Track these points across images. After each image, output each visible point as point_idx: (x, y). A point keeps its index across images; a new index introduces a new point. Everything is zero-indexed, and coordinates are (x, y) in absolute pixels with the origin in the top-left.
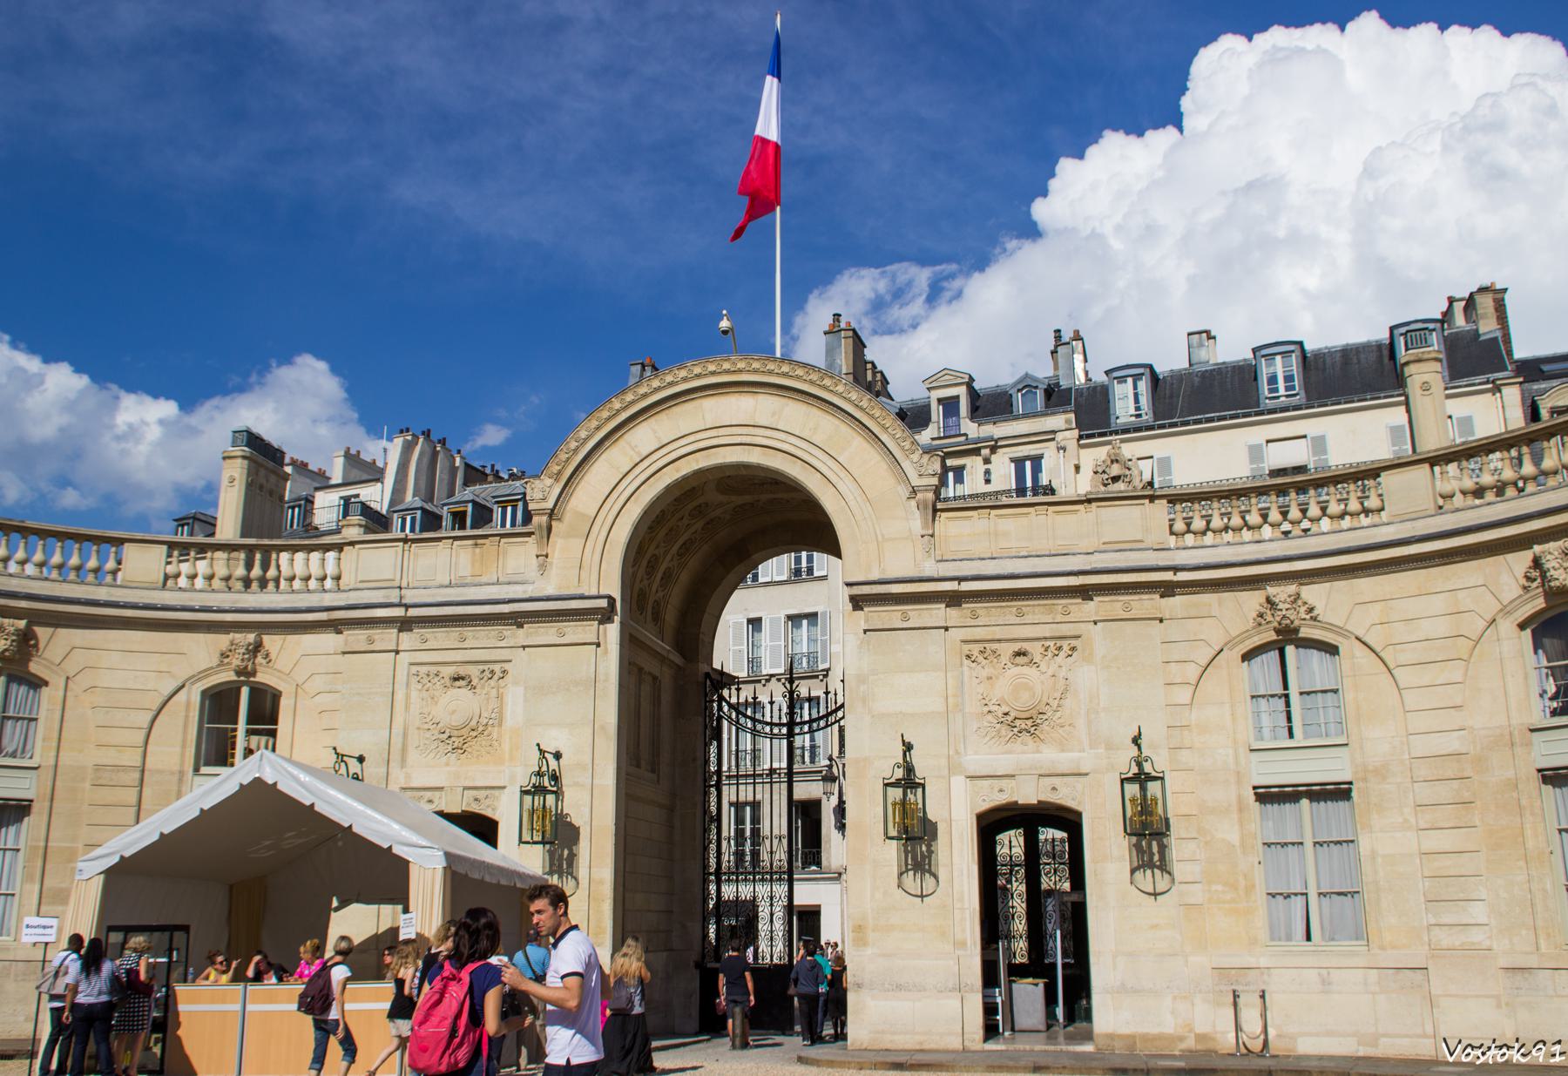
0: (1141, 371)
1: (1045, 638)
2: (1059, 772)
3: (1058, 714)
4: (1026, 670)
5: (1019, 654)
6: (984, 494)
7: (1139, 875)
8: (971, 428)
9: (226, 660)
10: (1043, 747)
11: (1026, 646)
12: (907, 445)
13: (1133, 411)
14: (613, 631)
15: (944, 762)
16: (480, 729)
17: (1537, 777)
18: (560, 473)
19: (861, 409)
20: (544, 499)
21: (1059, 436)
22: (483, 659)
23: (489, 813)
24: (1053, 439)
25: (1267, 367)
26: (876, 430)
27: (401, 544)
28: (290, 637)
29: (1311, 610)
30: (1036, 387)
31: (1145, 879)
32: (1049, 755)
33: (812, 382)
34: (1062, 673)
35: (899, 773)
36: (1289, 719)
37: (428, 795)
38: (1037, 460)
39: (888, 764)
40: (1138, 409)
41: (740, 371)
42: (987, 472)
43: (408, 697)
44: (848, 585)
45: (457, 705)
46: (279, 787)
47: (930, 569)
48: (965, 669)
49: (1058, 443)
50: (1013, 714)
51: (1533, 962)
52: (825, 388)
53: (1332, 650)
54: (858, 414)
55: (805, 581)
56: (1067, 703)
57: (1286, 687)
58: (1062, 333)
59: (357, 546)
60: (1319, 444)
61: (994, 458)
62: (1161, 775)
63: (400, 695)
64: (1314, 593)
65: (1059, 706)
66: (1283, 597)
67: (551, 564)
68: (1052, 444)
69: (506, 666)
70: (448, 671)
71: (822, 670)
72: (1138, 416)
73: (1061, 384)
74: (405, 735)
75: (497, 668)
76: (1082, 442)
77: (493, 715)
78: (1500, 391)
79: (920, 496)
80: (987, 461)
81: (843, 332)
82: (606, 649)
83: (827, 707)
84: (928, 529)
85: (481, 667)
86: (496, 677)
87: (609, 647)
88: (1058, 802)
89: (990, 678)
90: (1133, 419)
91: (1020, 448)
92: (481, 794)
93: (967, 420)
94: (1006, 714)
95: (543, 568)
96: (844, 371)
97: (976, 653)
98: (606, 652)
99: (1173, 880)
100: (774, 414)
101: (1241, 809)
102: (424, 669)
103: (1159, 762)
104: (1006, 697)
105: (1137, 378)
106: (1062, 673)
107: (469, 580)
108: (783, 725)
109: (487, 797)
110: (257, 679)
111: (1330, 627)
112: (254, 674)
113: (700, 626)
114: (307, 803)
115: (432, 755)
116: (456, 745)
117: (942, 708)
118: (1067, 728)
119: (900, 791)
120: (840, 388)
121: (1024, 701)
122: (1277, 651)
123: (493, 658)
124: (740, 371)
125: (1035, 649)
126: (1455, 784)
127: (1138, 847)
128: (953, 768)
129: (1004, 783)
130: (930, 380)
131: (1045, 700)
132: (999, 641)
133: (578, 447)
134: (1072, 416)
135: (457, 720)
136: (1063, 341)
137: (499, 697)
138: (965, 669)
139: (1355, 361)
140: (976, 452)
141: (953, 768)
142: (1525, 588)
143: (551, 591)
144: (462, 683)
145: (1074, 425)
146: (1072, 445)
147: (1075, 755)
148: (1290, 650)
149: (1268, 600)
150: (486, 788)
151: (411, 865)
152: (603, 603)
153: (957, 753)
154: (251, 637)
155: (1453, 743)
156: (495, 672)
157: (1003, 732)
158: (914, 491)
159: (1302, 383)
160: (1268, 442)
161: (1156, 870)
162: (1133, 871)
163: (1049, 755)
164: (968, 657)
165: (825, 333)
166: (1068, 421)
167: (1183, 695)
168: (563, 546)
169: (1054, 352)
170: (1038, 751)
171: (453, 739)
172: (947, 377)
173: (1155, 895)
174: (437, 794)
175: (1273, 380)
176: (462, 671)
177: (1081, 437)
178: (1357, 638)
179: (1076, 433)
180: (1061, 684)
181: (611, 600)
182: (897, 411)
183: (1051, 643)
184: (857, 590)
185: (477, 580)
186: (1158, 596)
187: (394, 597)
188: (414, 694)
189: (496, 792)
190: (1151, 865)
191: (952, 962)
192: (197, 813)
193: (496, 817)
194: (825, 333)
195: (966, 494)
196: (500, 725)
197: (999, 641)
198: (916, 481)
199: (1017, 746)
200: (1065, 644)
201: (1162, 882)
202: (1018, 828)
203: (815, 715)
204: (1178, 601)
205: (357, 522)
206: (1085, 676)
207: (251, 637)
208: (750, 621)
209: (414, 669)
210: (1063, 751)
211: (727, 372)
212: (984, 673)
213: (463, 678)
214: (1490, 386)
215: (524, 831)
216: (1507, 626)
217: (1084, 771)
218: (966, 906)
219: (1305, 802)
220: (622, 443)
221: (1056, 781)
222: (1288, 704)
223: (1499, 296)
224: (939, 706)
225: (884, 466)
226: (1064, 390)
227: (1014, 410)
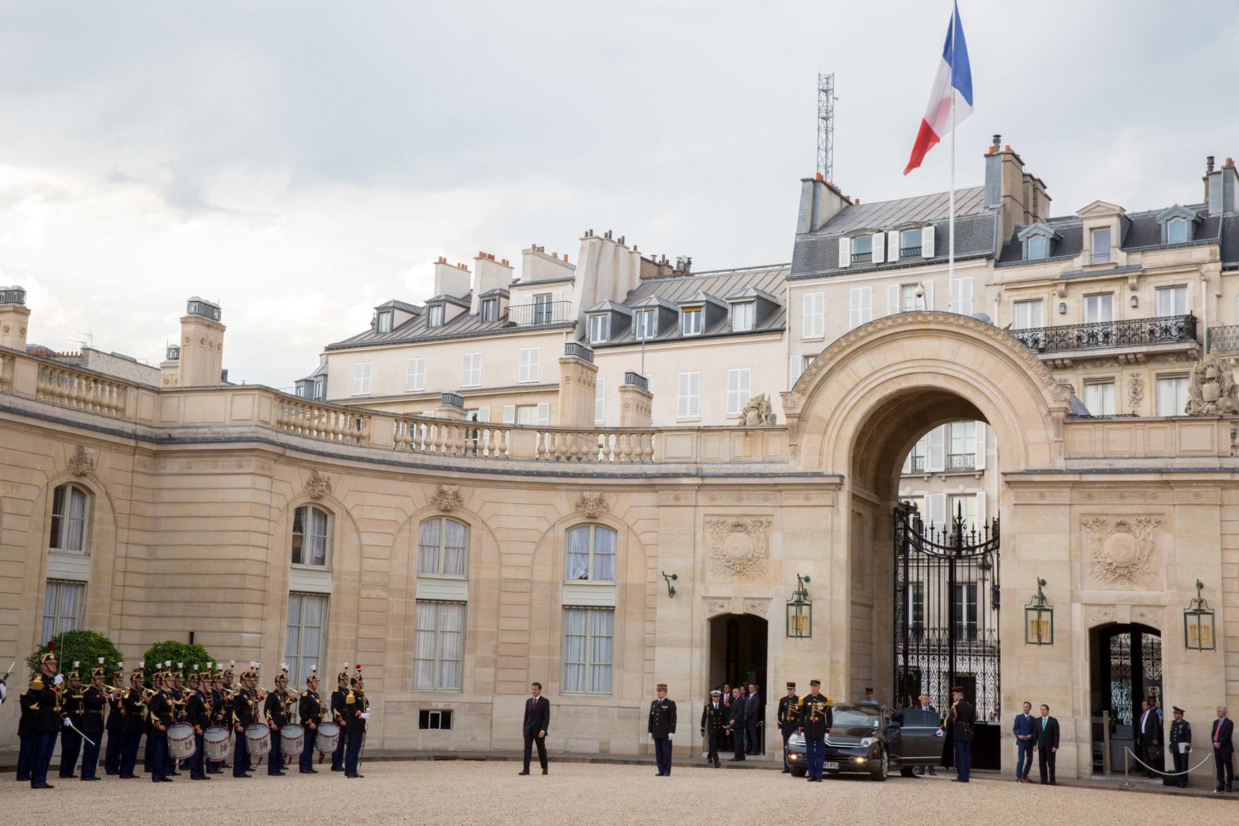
1: (1139, 515)
2: (1146, 604)
3: (1147, 566)
4: (1124, 535)
5: (1121, 524)
6: (1129, 321)
8: (1120, 257)
10: (1135, 586)
11: (1126, 519)
12: (1046, 379)
14: (843, 499)
15: (1068, 594)
16: (754, 560)
18: (805, 389)
21: (1204, 268)
22: (755, 513)
23: (761, 615)
26: (1024, 368)
27: (695, 433)
28: (621, 495)
32: (1139, 592)
33: (980, 332)
34: (1151, 538)
35: (1036, 602)
37: (720, 602)
39: (1028, 593)
41: (929, 322)
43: (704, 536)
44: (1004, 474)
45: (739, 544)
47: (1060, 464)
50: (1115, 565)
54: (1012, 356)
56: (1153, 558)
58: (1215, 160)
59: (664, 433)
62: (1212, 612)
63: (699, 536)
65: (1147, 560)
67: (800, 451)
68: (1196, 275)
69: (770, 519)
70: (731, 520)
73: (1210, 212)
74: (703, 562)
75: (764, 519)
76: (1223, 274)
77: (763, 551)
79: (1054, 414)
81: (1002, 156)
82: (838, 509)
83: (986, 538)
84: (1059, 437)
85: (754, 519)
86: (764, 526)
87: (840, 508)
88: (1145, 623)
89: (1099, 540)
91: (1166, 278)
92: (756, 603)
93: (1118, 250)
94: (1110, 564)
95: (794, 453)
96: (1003, 193)
98: (838, 511)
100: (953, 352)
103: (1213, 598)
104: (1110, 553)
106: (1151, 538)
109: (760, 604)
113: (891, 473)
115: (722, 576)
116: (738, 569)
117: (1066, 558)
118: (1152, 575)
119: (1036, 612)
120: (1000, 337)
121: (1121, 557)
123: (762, 513)
125: (1132, 521)
128: (1073, 599)
129: (1107, 610)
130: (1083, 211)
131: (1137, 555)
133: (817, 372)
135: (738, 554)
136: (1215, 170)
137: (767, 539)
138: (1083, 532)
141: (1073, 599)
143: (800, 469)
144: (739, 529)
145: (1218, 257)
146: (1215, 276)
147: (1158, 593)
150: (759, 599)
152: (837, 480)
153: (1076, 588)
154: (597, 494)
156: (764, 523)
157: (1108, 576)
158: (1050, 412)
163: (1139, 592)
165: (986, 156)
166: (1212, 253)
168: (808, 441)
169: (1205, 179)
170: (1132, 590)
171: (736, 566)
172: (1099, 209)
174: (726, 601)
176: (740, 521)
177: (1224, 269)
179: (1219, 265)
180: (1148, 548)
181: (842, 477)
182: (1052, 237)
183: (1143, 518)
184: (1009, 478)
186: (1219, 490)
187: (692, 469)
188: (708, 535)
189: (766, 602)
191: (1070, 723)
193: (766, 618)
194: (986, 156)
195: (1114, 320)
197: (1107, 515)
198: (1052, 405)
199: (1118, 585)
200: (1155, 520)
202: (1127, 633)
205: (631, 389)
206: (1166, 541)
207: (597, 494)
209: (708, 519)
210: (1149, 590)
211: (921, 322)
212: (1097, 535)
213: (742, 526)
215: (790, 629)
217: (1163, 603)
218: (1081, 688)
220: (848, 369)
221: (1144, 610)
224: (1064, 556)
226: (1211, 219)
227: (1163, 238)
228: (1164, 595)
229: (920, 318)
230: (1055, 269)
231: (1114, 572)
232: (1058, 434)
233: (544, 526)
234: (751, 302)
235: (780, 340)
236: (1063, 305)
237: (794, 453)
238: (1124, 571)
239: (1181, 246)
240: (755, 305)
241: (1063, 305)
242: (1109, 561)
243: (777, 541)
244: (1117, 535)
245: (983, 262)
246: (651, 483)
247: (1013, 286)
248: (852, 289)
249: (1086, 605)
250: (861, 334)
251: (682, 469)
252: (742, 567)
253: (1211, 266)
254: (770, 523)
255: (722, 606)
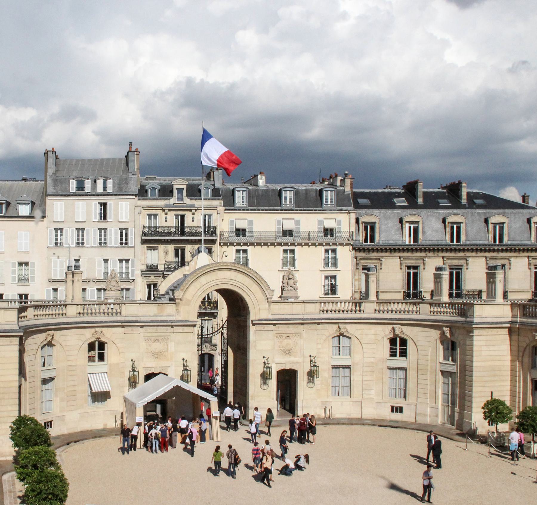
0: (245, 189)
1: (293, 333)
4: (289, 340)
7: (308, 384)
8: (187, 201)
9: (94, 336)
13: (241, 203)
17: (387, 368)
19: (257, 278)
20: (179, 296)
21: (218, 209)
24: (216, 210)
25: (284, 194)
29: (347, 330)
30: (209, 188)
31: (309, 385)
32: (292, 359)
33: (246, 270)
36: (339, 351)
38: (210, 216)
40: (243, 202)
41: (228, 266)
42: (193, 218)
45: (157, 347)
46: (181, 386)
48: (276, 339)
49: (218, 211)
51: (381, 401)
52: (249, 272)
53: (350, 338)
55: (124, 247)
57: (339, 345)
60: (298, 223)
61: (196, 213)
64: (348, 326)
66: (342, 327)
69: (169, 337)
71: (132, 280)
72: (243, 204)
75: (166, 337)
76: (225, 211)
78: (350, 214)
80: (193, 214)
89: (281, 342)
90: (241, 205)
94: (284, 350)
95: (178, 312)
96: (136, 168)
97: (278, 337)
98: (194, 334)
99: (315, 385)
101: (329, 369)
102: (147, 338)
105: (243, 191)
107: (157, 314)
108: (200, 335)
110: (101, 340)
111: (350, 334)
112: (100, 338)
114: (188, 390)
121: (288, 347)
122: (338, 337)
124: (228, 266)
125: (291, 335)
126: (371, 368)
127: (308, 378)
132: (283, 333)
134: (222, 201)
137: (167, 345)
139: (309, 194)
140: (191, 210)
142: (390, 332)
143: (180, 319)
144: (157, 341)
148: (341, 337)
149: (339, 327)
151: (211, 401)
155: (372, 360)
159: (294, 201)
160: (283, 219)
161: (312, 383)
162: (307, 383)
163: (292, 359)
164: (277, 337)
166: (220, 203)
167: (320, 346)
168: (183, 308)
170: (290, 358)
173: (311, 388)
174: (152, 368)
175: (286, 199)
176: (157, 338)
178: (356, 337)
183: (294, 334)
185: (160, 315)
189: (167, 368)
190: (311, 382)
192: (164, 393)
196: (167, 351)
197: (283, 333)
201: (312, 385)
203: (209, 333)
204: (320, 325)
208: (104, 260)
211: (225, 266)
214: (347, 212)
216: (385, 339)
219: (341, 369)
222: (339, 348)
223: (373, 225)
225: (260, 292)
228: (300, 360)
229: (225, 264)
230: (162, 203)
231: (285, 352)
232: (269, 306)
233: (81, 343)
234: (29, 203)
235: (43, 221)
236: (166, 218)
237: (178, 312)
238: (288, 352)
239: (209, 199)
240: (30, 205)
241: (166, 218)
242: (284, 349)
243: (171, 346)
244: (286, 340)
245: (134, 197)
246: (123, 325)
247: (145, 208)
248: (77, 202)
249: (276, 364)
250: (204, 269)
251: (134, 319)
252: (158, 355)
253: (221, 208)
254: (168, 338)
255: (150, 370)
